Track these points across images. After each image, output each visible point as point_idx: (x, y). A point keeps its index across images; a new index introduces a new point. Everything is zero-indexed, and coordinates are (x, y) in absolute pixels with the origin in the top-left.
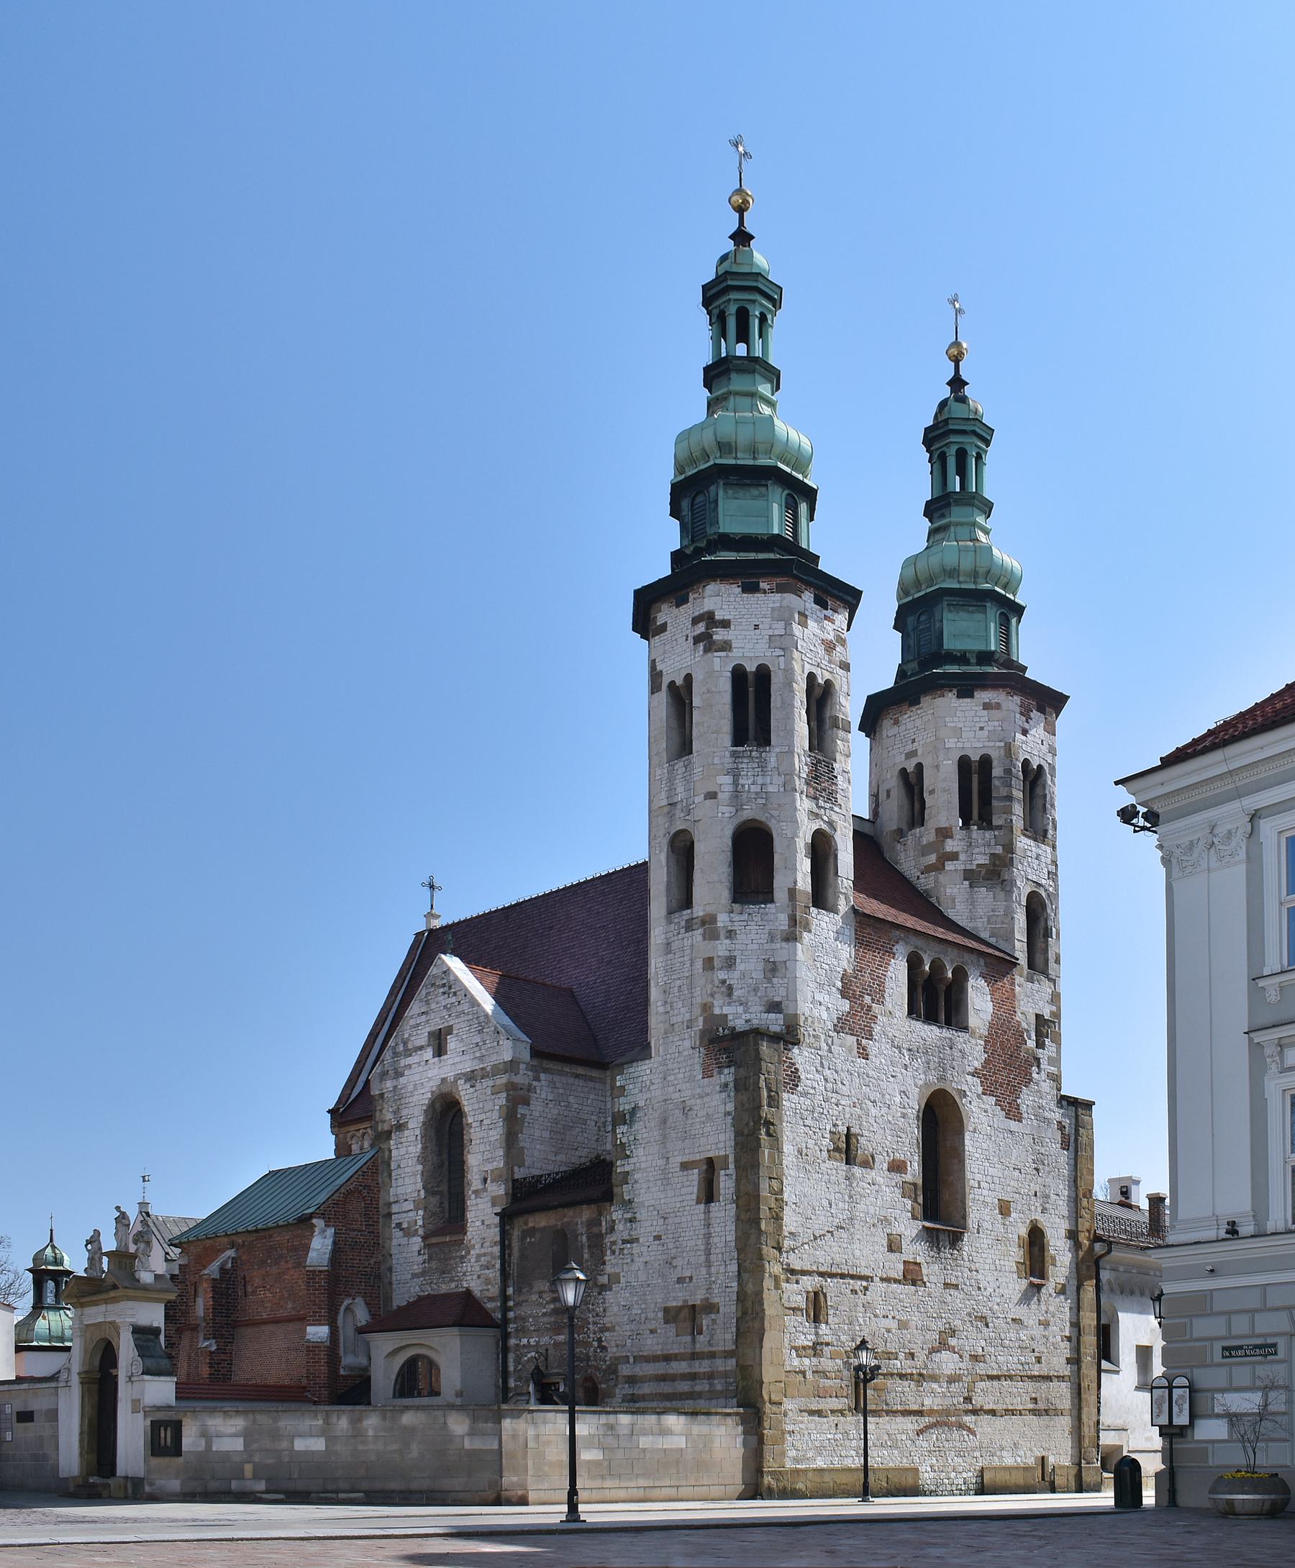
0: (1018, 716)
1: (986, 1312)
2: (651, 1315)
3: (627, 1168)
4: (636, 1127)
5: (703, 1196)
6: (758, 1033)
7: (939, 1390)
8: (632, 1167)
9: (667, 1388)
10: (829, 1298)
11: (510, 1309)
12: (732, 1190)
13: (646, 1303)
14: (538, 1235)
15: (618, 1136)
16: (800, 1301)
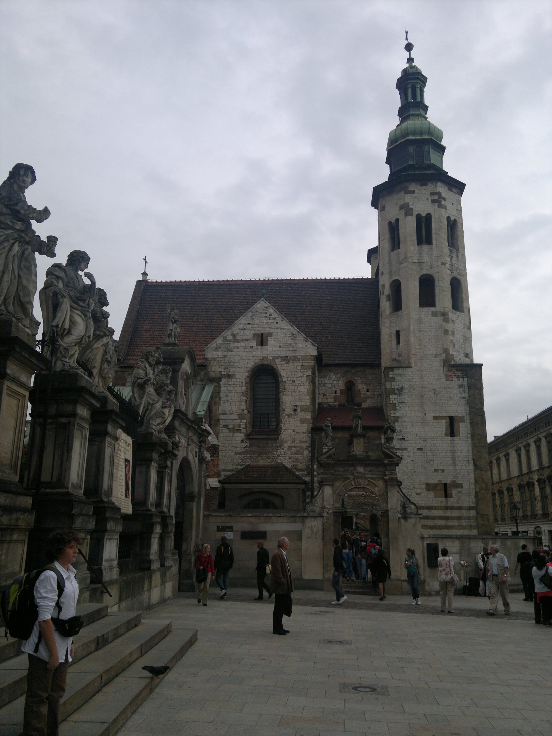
2: (417, 486)
3: (397, 415)
4: (403, 397)
5: (449, 432)
8: (402, 415)
11: (315, 476)
15: (391, 399)
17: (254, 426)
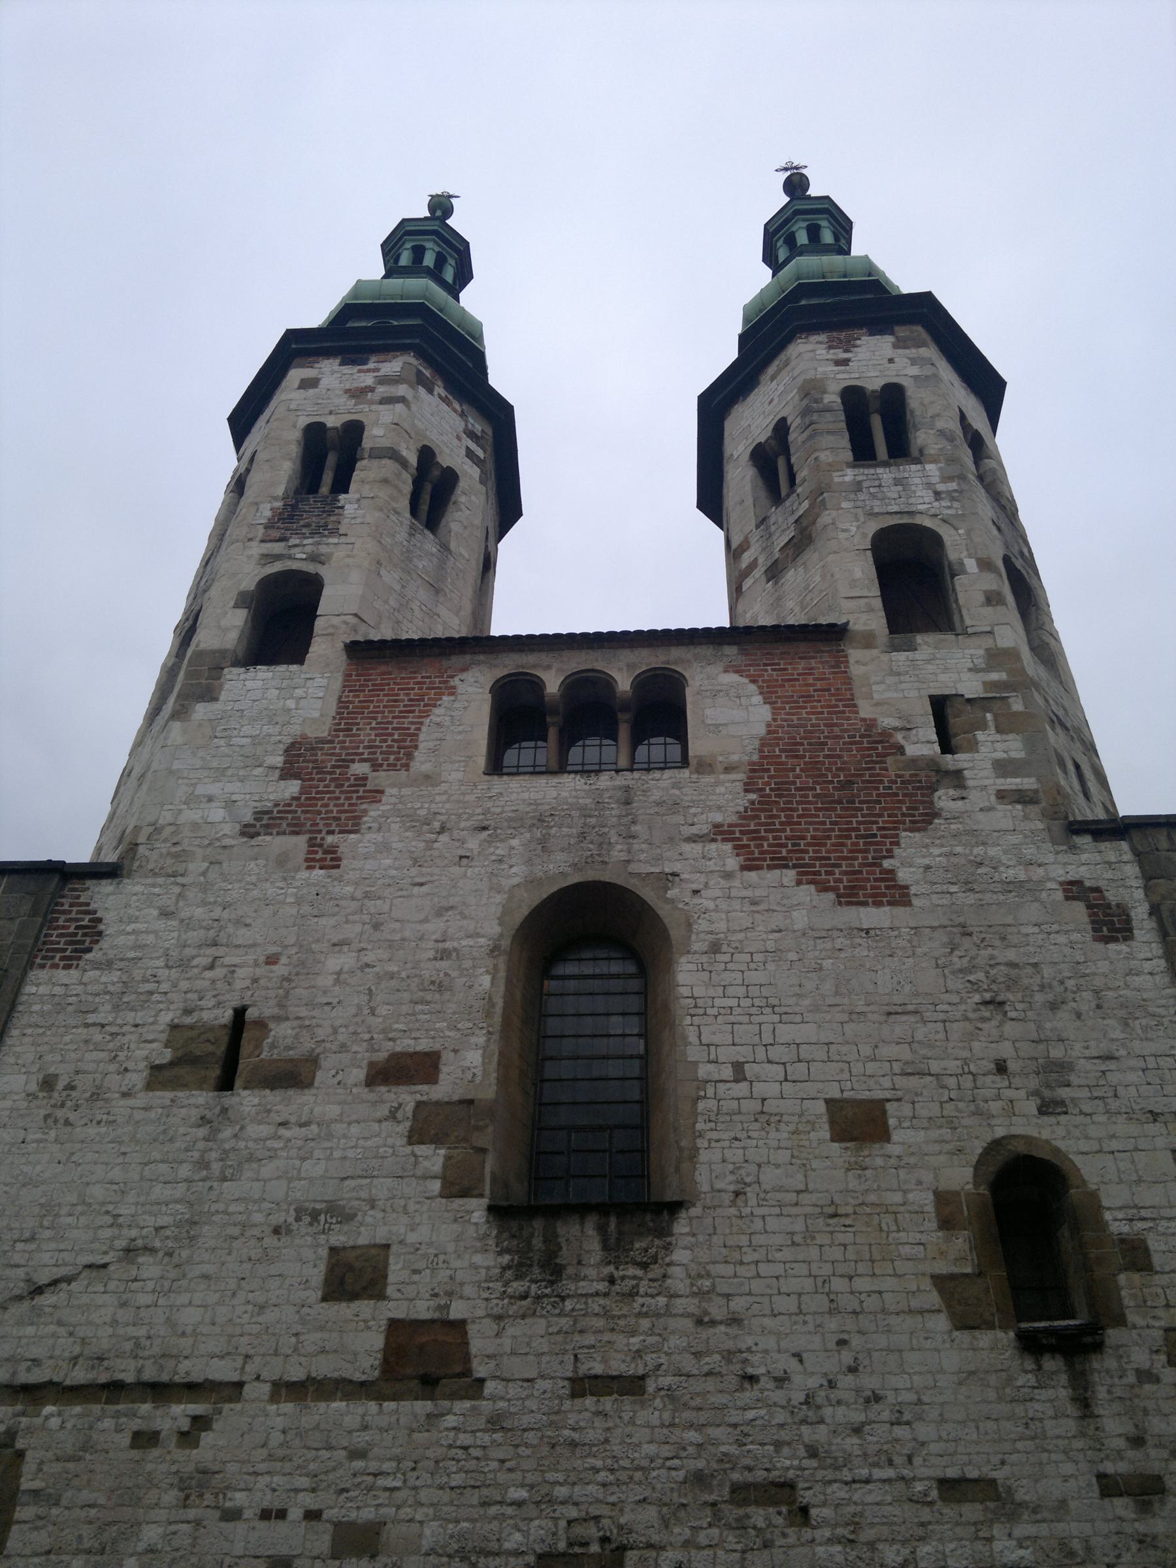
1: (786, 1464)
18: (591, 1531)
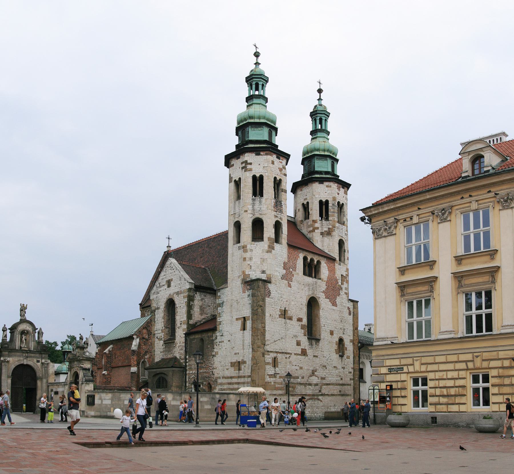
0: (336, 189)
2: (227, 364)
3: (221, 320)
4: (223, 308)
5: (242, 328)
6: (258, 280)
7: (312, 388)
8: (222, 320)
9: (231, 386)
10: (279, 360)
12: (251, 327)
13: (225, 361)
14: (195, 340)
16: (270, 360)
17: (171, 336)
18: (315, 368)
